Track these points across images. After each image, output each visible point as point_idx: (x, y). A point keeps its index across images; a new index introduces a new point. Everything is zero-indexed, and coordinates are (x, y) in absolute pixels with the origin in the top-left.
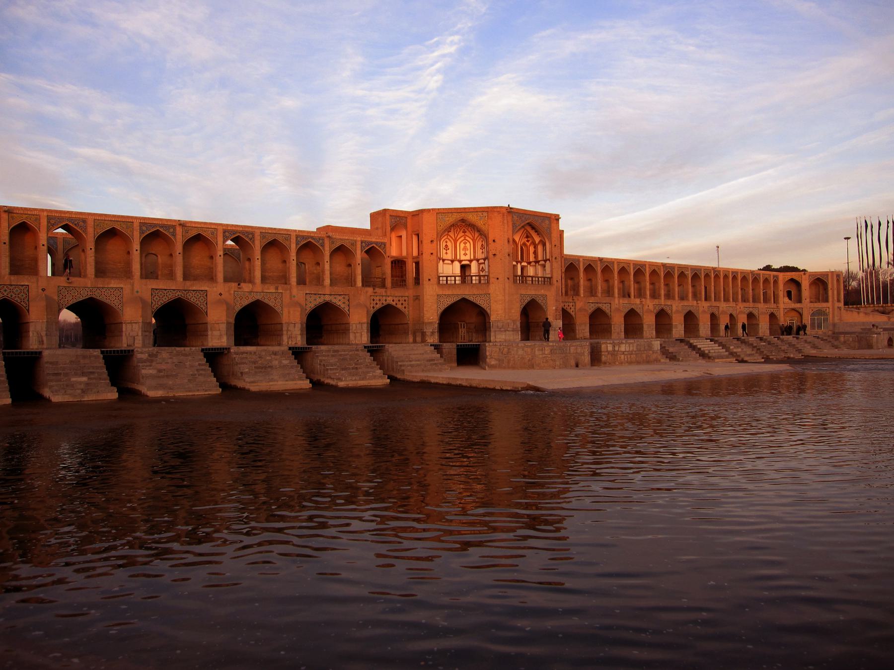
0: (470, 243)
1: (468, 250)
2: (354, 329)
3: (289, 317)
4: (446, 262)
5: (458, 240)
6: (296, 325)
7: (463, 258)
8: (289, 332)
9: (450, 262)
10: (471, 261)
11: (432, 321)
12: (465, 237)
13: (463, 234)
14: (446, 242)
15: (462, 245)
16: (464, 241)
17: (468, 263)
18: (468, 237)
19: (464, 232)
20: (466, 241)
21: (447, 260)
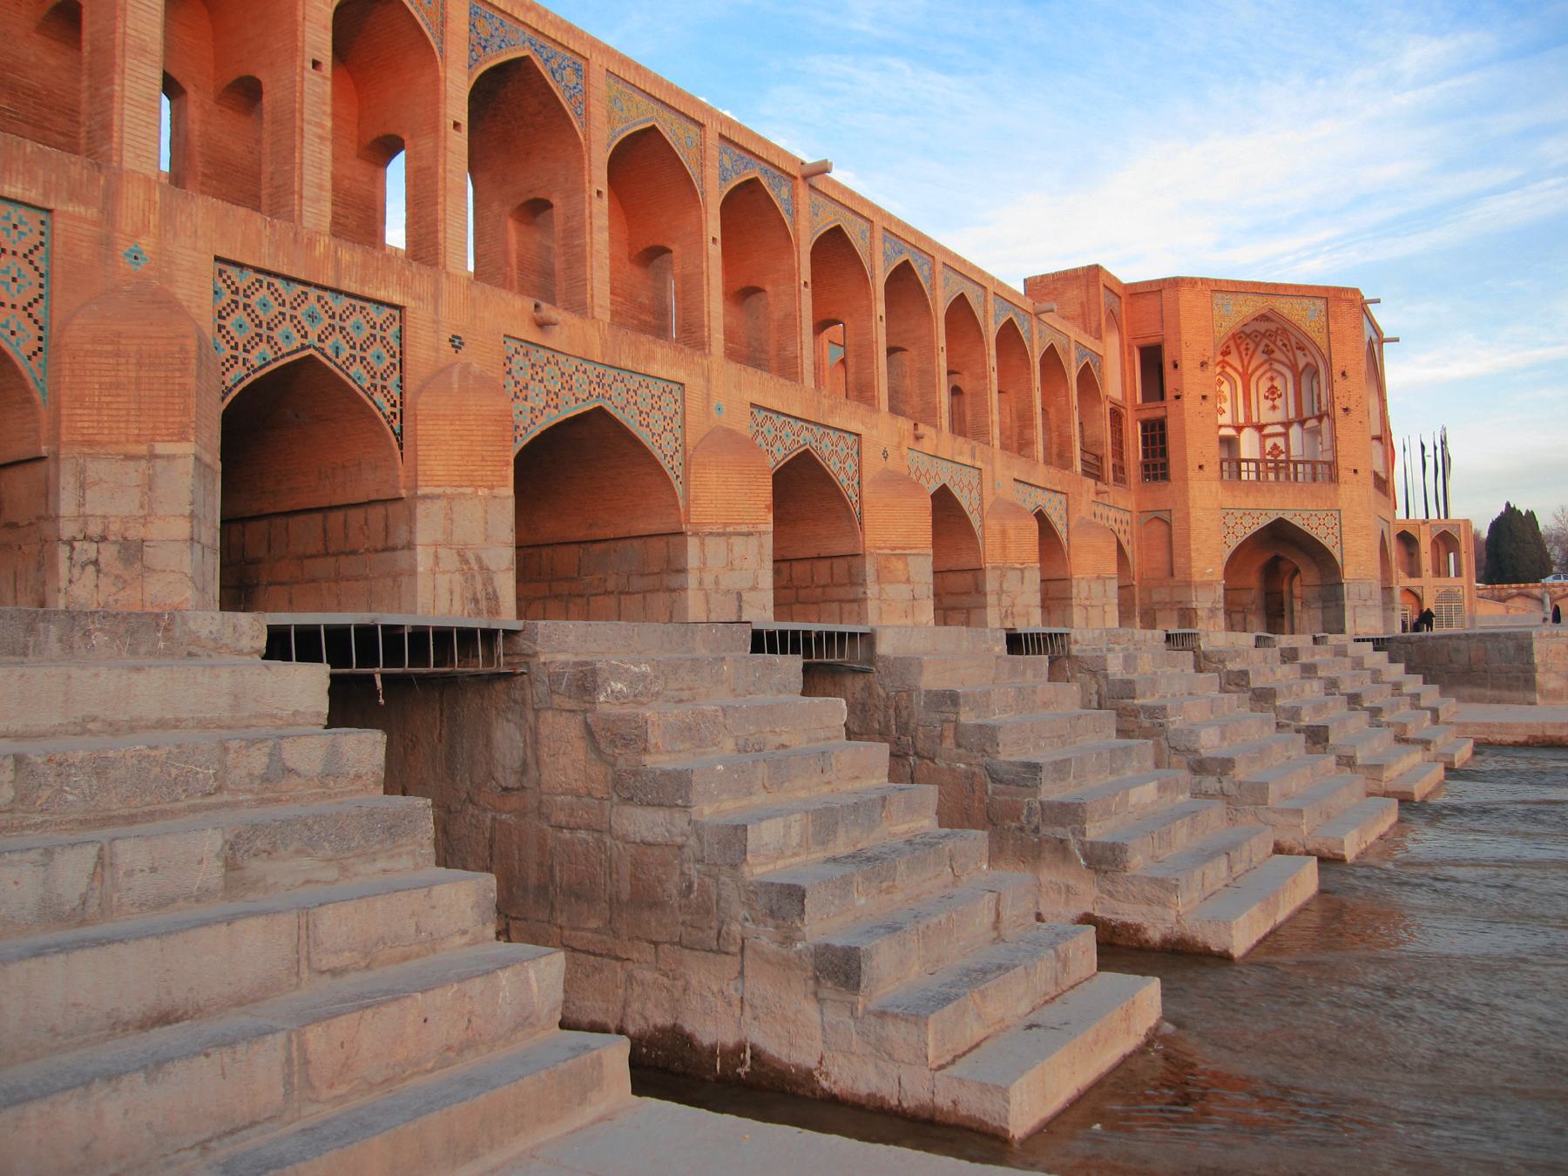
0: (1285, 377)
1: (1280, 396)
2: (1084, 595)
3: (1004, 548)
6: (1027, 574)
8: (1004, 597)
11: (1210, 578)
13: (1265, 357)
15: (1264, 386)
16: (1269, 374)
19: (1268, 352)
20: (1275, 375)
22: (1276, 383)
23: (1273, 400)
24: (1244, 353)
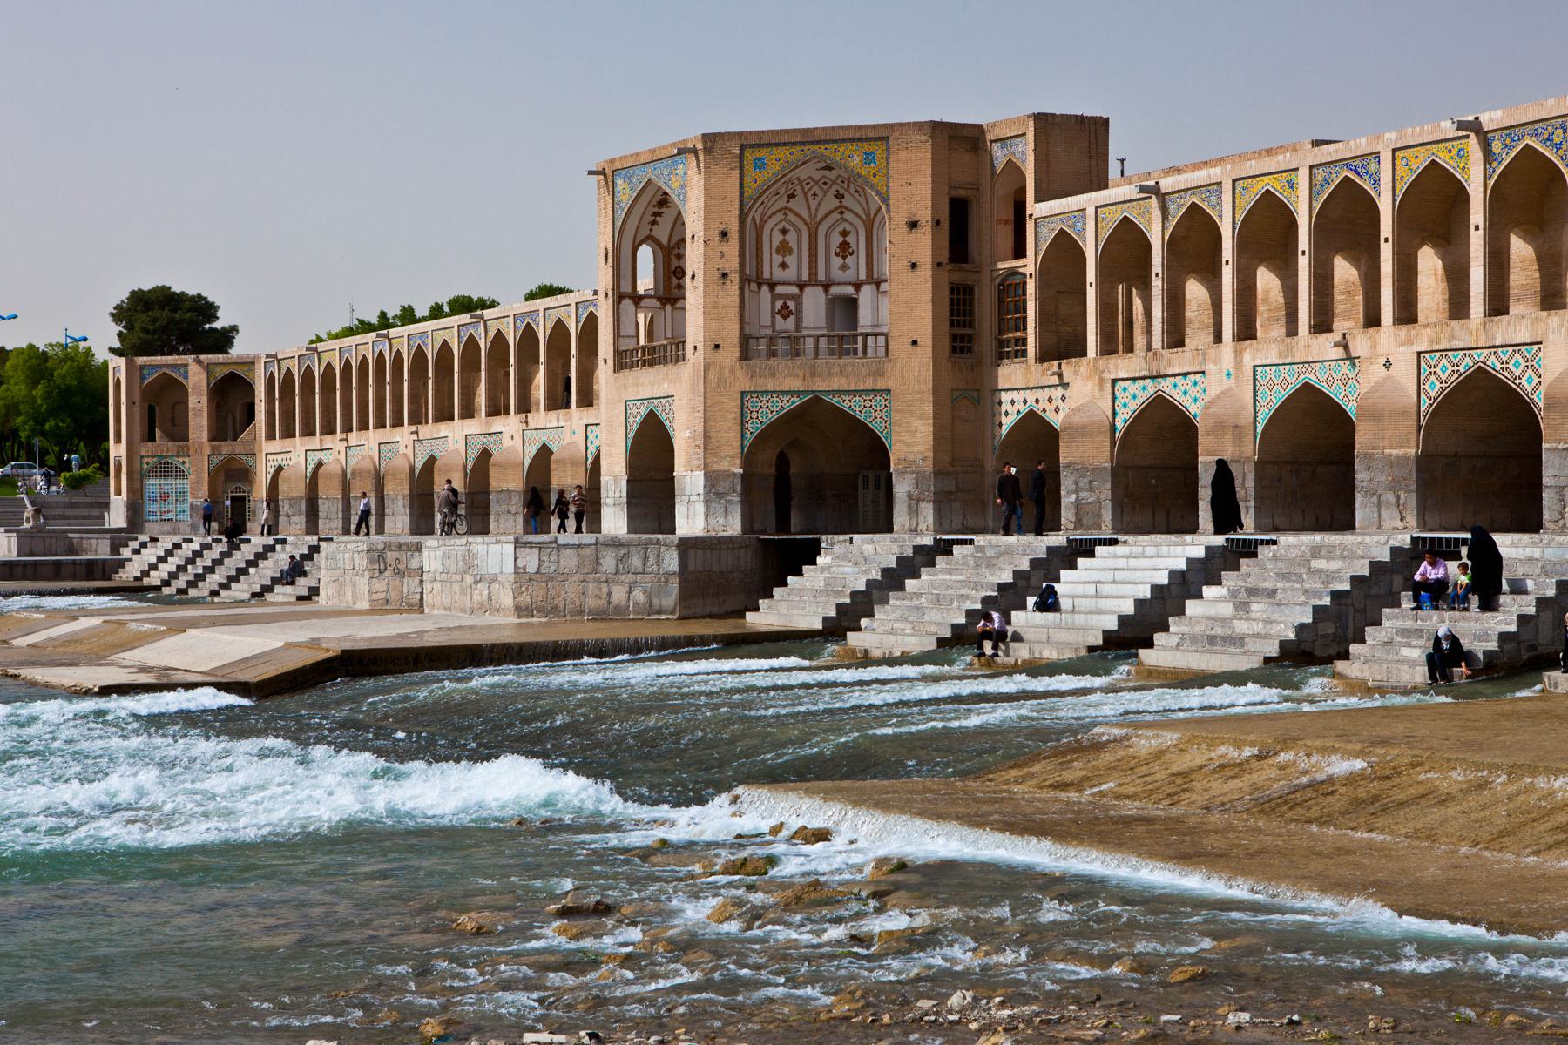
1: (851, 254)
4: (779, 289)
5: (822, 220)
7: (837, 274)
9: (794, 290)
10: (858, 286)
12: (842, 213)
13: (836, 202)
14: (784, 232)
15: (836, 240)
17: (850, 290)
18: (851, 211)
19: (839, 196)
21: (784, 283)
22: (847, 239)
23: (844, 257)
24: (810, 198)
